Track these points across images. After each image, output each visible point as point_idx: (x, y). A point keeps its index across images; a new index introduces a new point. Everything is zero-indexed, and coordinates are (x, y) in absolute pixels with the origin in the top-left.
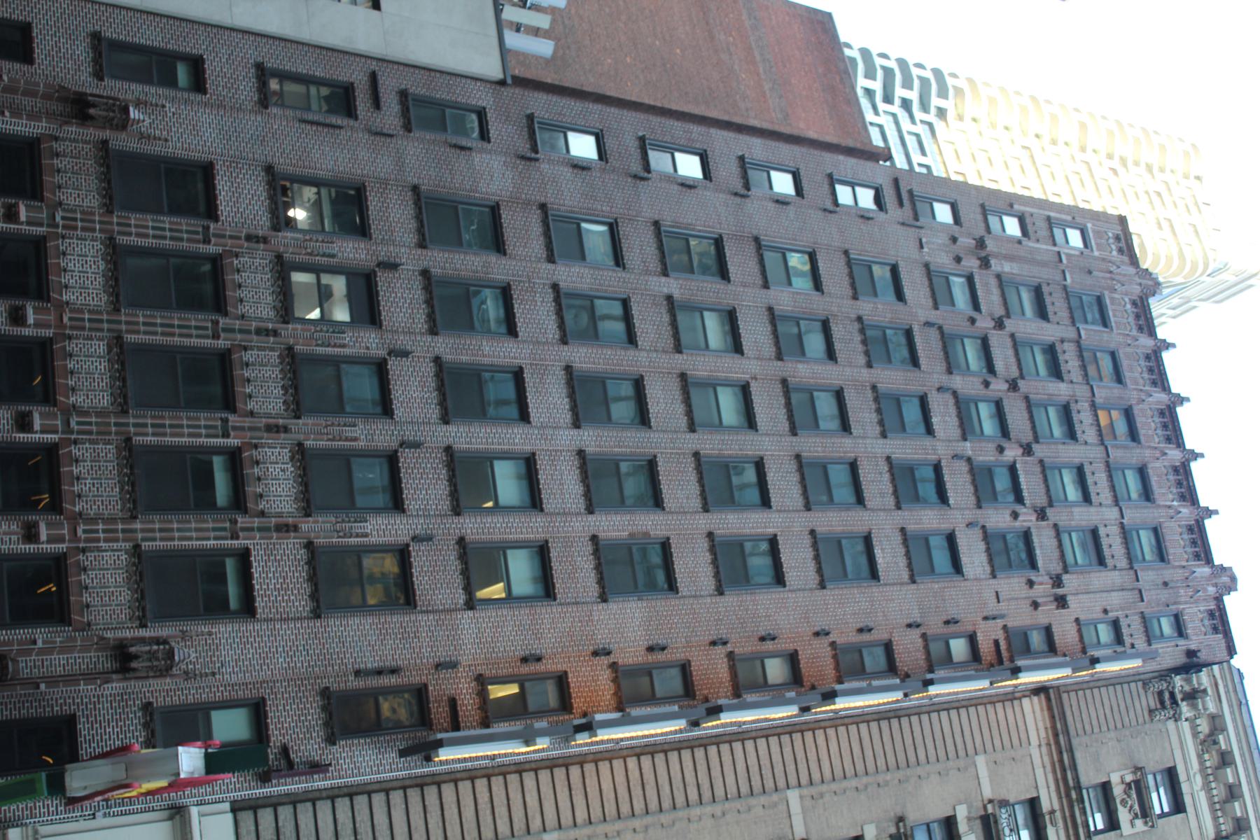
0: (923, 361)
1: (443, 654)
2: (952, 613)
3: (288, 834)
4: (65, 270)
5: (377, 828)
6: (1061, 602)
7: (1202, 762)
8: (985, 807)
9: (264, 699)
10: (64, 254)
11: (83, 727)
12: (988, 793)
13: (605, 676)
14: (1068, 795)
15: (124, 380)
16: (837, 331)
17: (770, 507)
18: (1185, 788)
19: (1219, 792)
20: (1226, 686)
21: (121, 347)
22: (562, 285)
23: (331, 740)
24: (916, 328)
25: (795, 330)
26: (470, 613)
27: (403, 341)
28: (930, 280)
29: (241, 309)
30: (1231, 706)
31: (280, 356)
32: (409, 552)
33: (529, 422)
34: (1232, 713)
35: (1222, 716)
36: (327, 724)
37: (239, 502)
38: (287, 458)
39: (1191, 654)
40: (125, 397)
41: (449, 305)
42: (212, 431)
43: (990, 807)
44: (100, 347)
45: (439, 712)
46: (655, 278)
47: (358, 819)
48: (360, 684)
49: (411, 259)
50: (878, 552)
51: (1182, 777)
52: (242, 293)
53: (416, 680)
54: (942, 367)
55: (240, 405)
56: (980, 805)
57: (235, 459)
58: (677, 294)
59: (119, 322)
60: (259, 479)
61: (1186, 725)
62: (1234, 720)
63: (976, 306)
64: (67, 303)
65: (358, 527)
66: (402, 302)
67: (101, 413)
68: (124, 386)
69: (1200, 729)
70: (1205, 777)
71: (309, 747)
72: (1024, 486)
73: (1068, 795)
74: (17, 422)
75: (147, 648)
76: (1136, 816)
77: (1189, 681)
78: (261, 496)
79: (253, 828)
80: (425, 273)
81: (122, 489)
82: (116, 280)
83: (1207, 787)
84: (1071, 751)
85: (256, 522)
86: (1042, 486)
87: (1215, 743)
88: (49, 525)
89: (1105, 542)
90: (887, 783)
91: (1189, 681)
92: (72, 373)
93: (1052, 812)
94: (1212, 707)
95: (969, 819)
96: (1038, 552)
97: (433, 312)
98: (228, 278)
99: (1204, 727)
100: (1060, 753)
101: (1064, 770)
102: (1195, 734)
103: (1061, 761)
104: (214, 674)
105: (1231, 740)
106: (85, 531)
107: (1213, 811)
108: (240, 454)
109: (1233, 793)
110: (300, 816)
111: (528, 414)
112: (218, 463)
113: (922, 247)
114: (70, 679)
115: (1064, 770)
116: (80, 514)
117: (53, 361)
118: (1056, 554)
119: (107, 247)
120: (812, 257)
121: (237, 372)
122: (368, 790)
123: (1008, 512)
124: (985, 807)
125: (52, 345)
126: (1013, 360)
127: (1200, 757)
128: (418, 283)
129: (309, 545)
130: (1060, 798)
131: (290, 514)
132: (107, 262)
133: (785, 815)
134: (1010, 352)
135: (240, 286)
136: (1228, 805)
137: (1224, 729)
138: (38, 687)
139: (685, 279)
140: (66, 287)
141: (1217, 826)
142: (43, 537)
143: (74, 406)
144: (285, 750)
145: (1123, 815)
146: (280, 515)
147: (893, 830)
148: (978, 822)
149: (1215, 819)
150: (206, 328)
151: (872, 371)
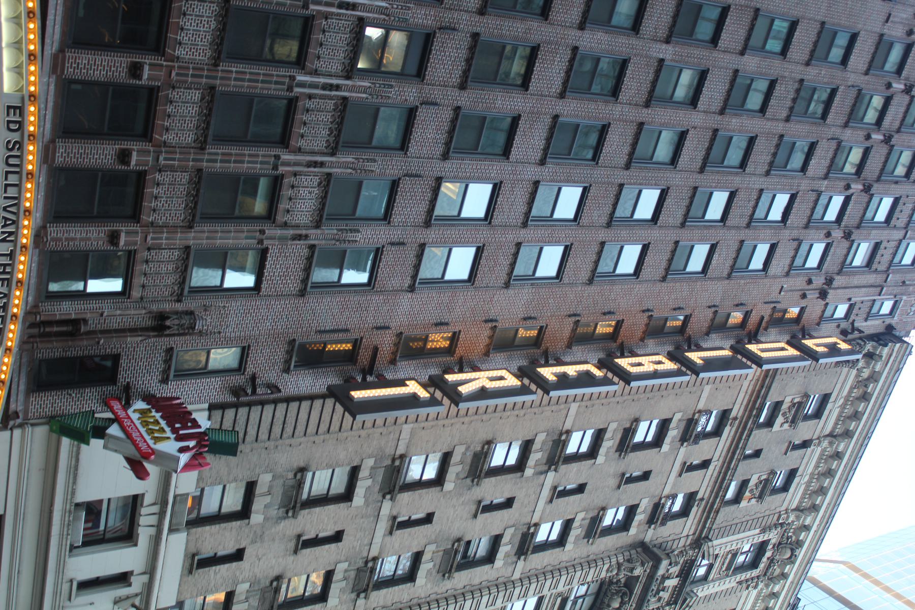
0: (831, 116)
1: (380, 322)
2: (744, 299)
3: (241, 423)
4: (182, 29)
5: (299, 420)
6: (823, 294)
7: (850, 392)
8: (694, 414)
9: (249, 346)
10: (185, 14)
11: (123, 362)
12: (701, 406)
13: (487, 333)
14: (751, 411)
15: (208, 124)
16: (779, 90)
17: (656, 224)
18: (829, 406)
19: (849, 410)
20: (896, 357)
21: (213, 96)
22: (581, 50)
23: (287, 370)
24: (841, 89)
25: (749, 82)
26: (410, 295)
27: (436, 94)
28: (877, 48)
29: (317, 64)
30: (891, 369)
31: (335, 104)
32: (382, 251)
33: (508, 158)
34: (889, 373)
35: (880, 374)
36: (288, 362)
37: (270, 215)
38: (316, 184)
39: (890, 328)
40: (206, 137)
41: (482, 63)
42: (266, 166)
43: (697, 415)
44: (196, 95)
45: (364, 357)
46: (658, 45)
47: (288, 415)
48: (318, 338)
49: (467, 22)
50: (716, 257)
51: (832, 399)
52: (322, 51)
53: (356, 336)
54: (841, 120)
55: (292, 143)
56: (692, 412)
57: (276, 183)
58: (668, 57)
59: (215, 78)
60: (290, 199)
61: (854, 372)
62: (887, 378)
63: (899, 71)
64: (178, 58)
65: (350, 236)
66: (448, 59)
67: (185, 149)
68: (207, 128)
69: (862, 374)
70: (847, 400)
71: (270, 374)
72: (847, 213)
73: (751, 411)
74: (119, 157)
75: (176, 322)
76: (787, 422)
77: (875, 348)
78: (288, 211)
79: (220, 420)
80: (475, 36)
81: (187, 206)
82: (222, 39)
83: (843, 407)
84: (769, 388)
85: (279, 232)
86: (862, 212)
87: (866, 386)
88: (128, 233)
89: (880, 252)
90: (639, 400)
91: (875, 348)
92: (169, 116)
93: (735, 419)
94: (878, 368)
95: (680, 420)
96: (828, 258)
97: (469, 70)
98: (314, 37)
99: (866, 374)
100: (762, 387)
101: (757, 397)
102: (858, 376)
103: (759, 391)
104: (220, 333)
105: (875, 390)
106: (153, 239)
107: (838, 420)
108: (282, 179)
109: (856, 416)
110: (252, 414)
111: (510, 151)
112: (263, 184)
113: (887, 21)
114: (122, 332)
115: (757, 397)
116: (152, 223)
117: (156, 105)
118: (841, 260)
119: (222, 8)
120: (793, 26)
121: (298, 116)
122: (300, 399)
123: (825, 231)
124: (694, 414)
125: (158, 92)
126: (901, 116)
127: (852, 388)
128: (466, 42)
129: (312, 247)
130: (745, 410)
131: (307, 227)
132: (220, 22)
133: (564, 416)
134: (903, 110)
135: (321, 45)
136: (848, 421)
137: (877, 381)
138: (98, 343)
139: (684, 44)
140: (180, 44)
141: (834, 428)
142: (122, 243)
143: (165, 142)
144: (253, 378)
145: (780, 419)
146: (297, 226)
147: (628, 425)
148: (685, 422)
149: (836, 424)
150: (283, 83)
151: (788, 125)
